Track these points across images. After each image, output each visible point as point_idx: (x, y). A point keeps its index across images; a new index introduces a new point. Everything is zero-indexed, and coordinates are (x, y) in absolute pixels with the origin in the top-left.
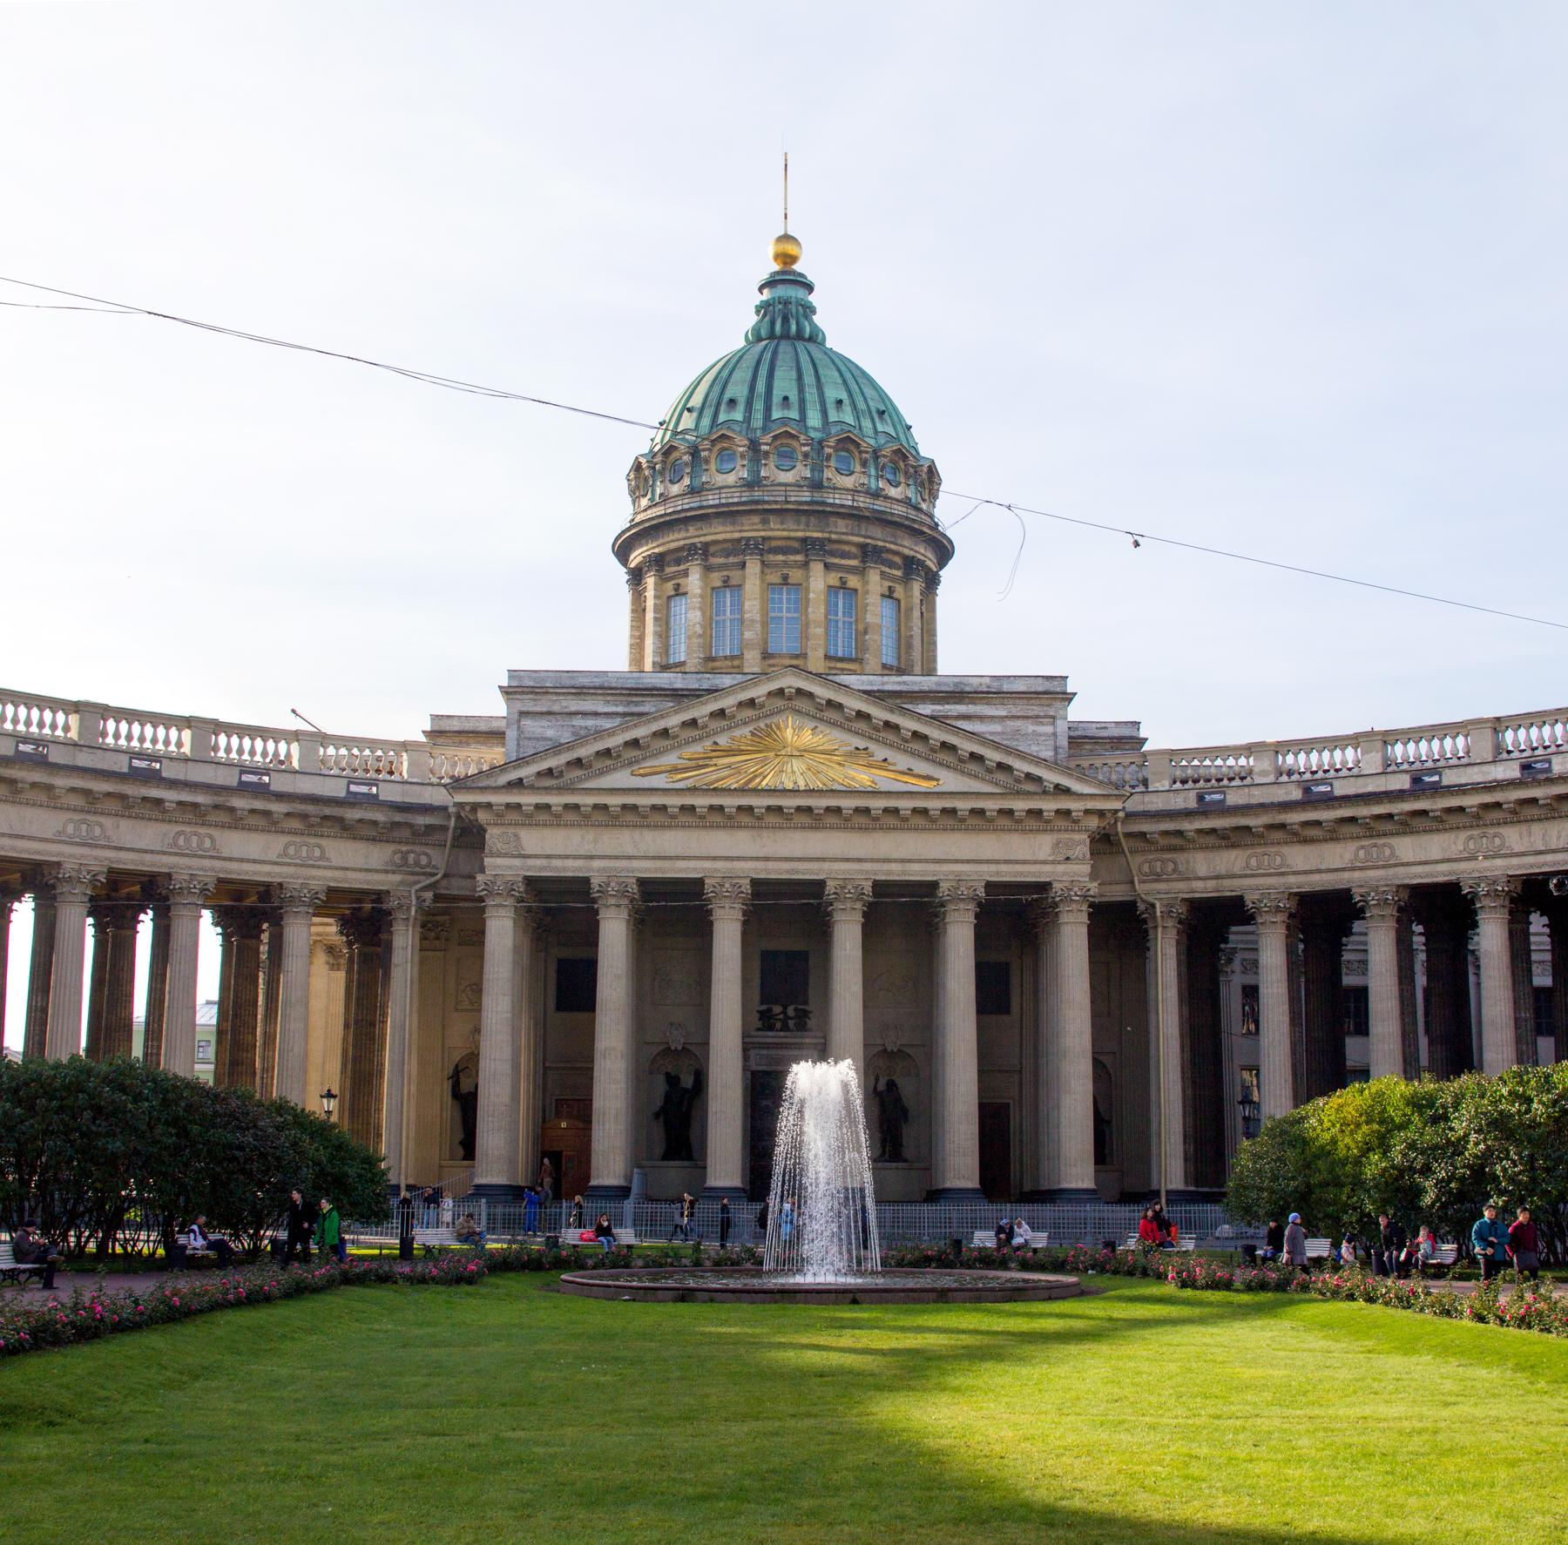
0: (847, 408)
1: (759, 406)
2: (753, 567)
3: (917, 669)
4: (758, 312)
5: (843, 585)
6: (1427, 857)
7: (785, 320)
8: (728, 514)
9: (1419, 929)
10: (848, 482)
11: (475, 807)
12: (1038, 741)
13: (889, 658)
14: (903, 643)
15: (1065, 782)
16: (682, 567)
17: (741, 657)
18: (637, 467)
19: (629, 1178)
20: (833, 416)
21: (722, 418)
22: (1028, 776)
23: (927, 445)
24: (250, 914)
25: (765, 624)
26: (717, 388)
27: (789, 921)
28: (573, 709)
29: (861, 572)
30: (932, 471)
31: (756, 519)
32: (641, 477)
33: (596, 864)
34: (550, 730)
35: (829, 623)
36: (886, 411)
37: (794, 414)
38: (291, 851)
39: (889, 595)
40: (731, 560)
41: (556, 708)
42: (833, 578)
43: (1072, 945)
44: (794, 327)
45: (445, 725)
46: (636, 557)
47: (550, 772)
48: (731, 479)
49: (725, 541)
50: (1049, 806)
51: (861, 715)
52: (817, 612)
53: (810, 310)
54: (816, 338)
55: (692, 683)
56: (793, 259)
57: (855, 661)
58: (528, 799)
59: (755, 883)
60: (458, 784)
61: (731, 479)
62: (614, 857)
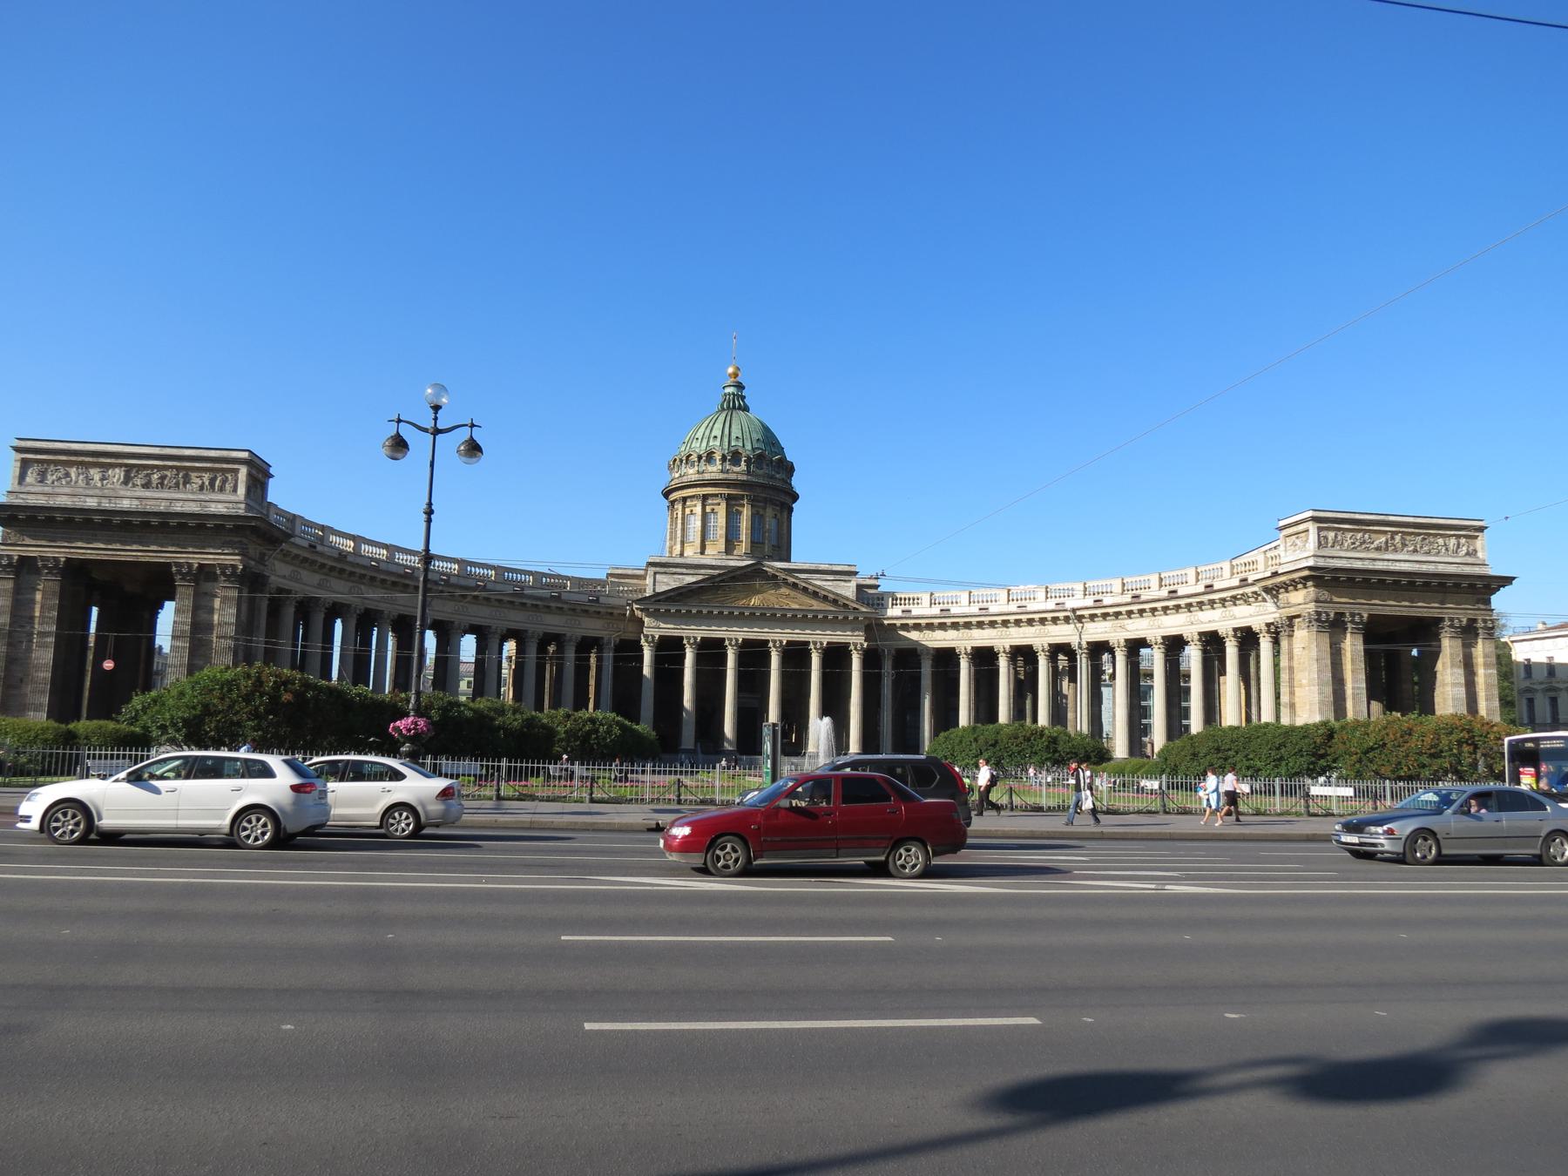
6: (982, 638)
12: (848, 590)
46: (673, 496)
54: (746, 409)
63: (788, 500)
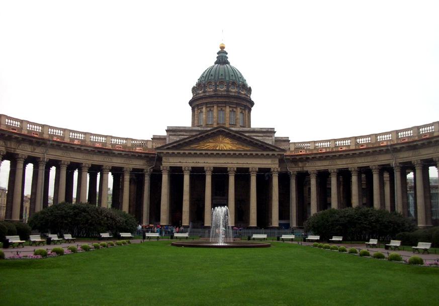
1: (217, 76)
2: (215, 107)
3: (247, 126)
4: (217, 57)
5: (233, 111)
6: (342, 164)
8: (210, 97)
9: (341, 177)
10: (234, 90)
11: (160, 153)
12: (269, 141)
13: (241, 124)
14: (244, 122)
15: (274, 148)
19: (189, 224)
23: (249, 84)
24: (118, 174)
25: (218, 118)
27: (220, 176)
29: (236, 108)
30: (250, 88)
32: (194, 90)
34: (176, 139)
35: (230, 118)
36: (242, 77)
39: (242, 112)
40: (212, 105)
41: (176, 134)
42: (231, 109)
45: (156, 137)
47: (174, 146)
50: (271, 153)
51: (235, 135)
52: (228, 115)
54: (228, 63)
55: (202, 129)
56: (224, 48)
57: (234, 125)
58: (171, 152)
59: (214, 168)
60: (158, 148)
61: (211, 90)
62: (187, 163)
63: (248, 104)
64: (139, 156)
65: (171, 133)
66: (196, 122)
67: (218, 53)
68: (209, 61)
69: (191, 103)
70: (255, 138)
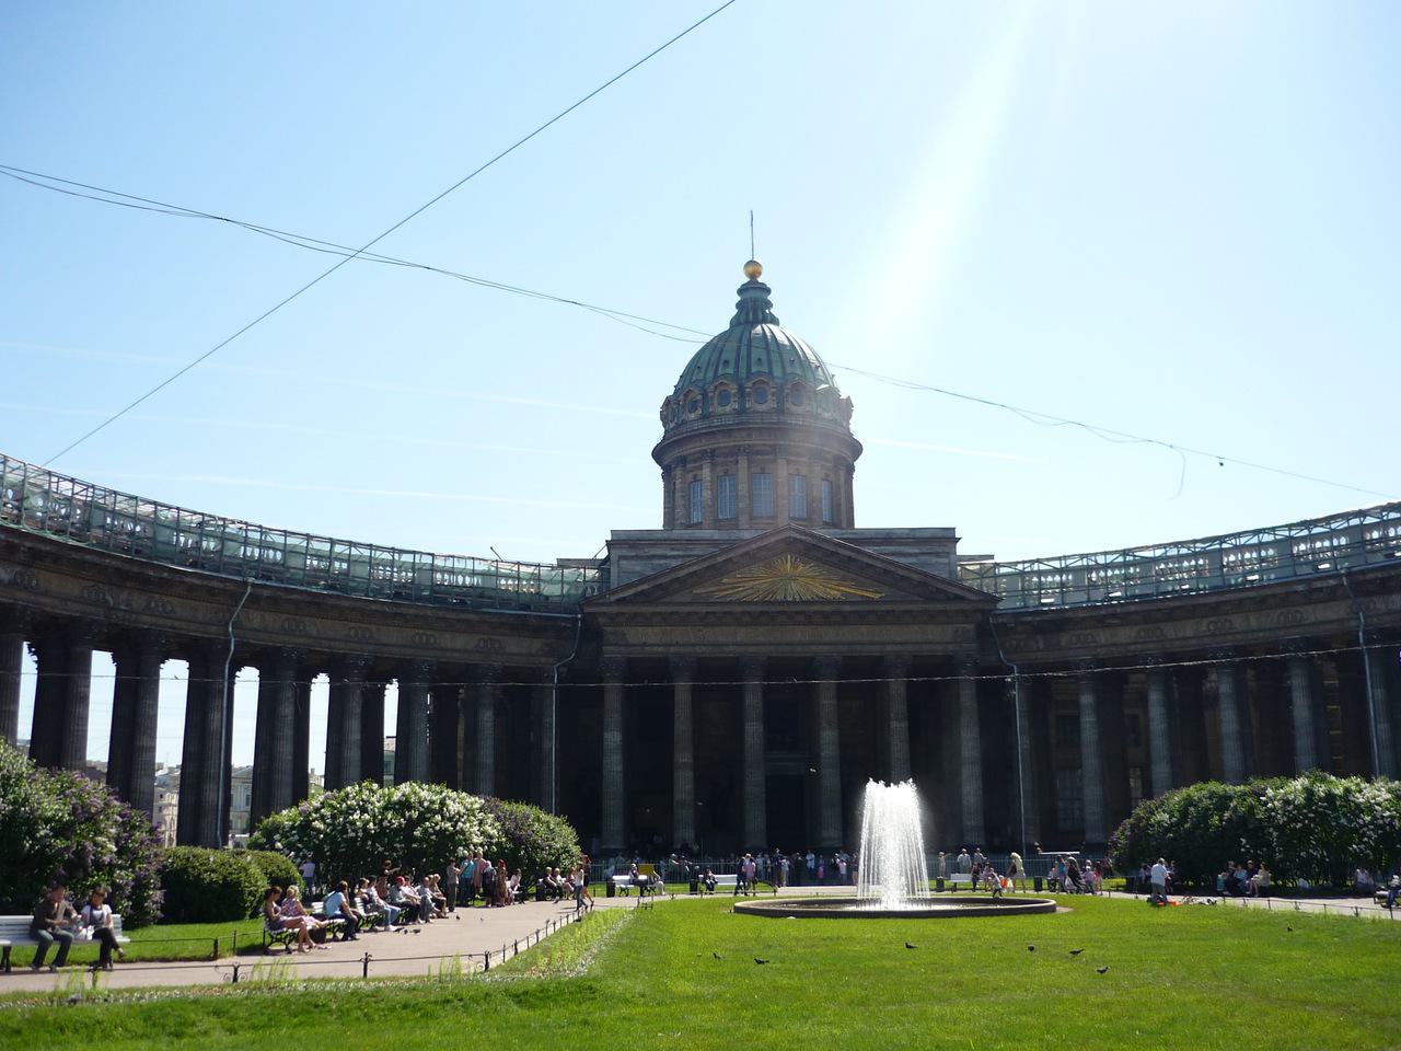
0: (797, 364)
1: (743, 364)
2: (743, 463)
4: (738, 306)
7: (755, 312)
13: (826, 518)
15: (959, 592)
16: (698, 464)
17: (737, 519)
18: (668, 401)
20: (789, 370)
21: (720, 372)
22: (939, 590)
25: (751, 497)
26: (716, 355)
28: (652, 553)
31: (744, 434)
33: (672, 649)
34: (637, 567)
37: (765, 369)
38: (481, 644)
40: (730, 459)
41: (641, 553)
43: (967, 698)
44: (761, 317)
46: (669, 458)
48: (728, 409)
49: (725, 447)
50: (951, 607)
53: (769, 305)
54: (775, 321)
61: (728, 409)
64: (519, 626)
65: (625, 552)
66: (680, 512)
67: (740, 292)
68: (718, 317)
69: (658, 454)
70: (902, 560)
